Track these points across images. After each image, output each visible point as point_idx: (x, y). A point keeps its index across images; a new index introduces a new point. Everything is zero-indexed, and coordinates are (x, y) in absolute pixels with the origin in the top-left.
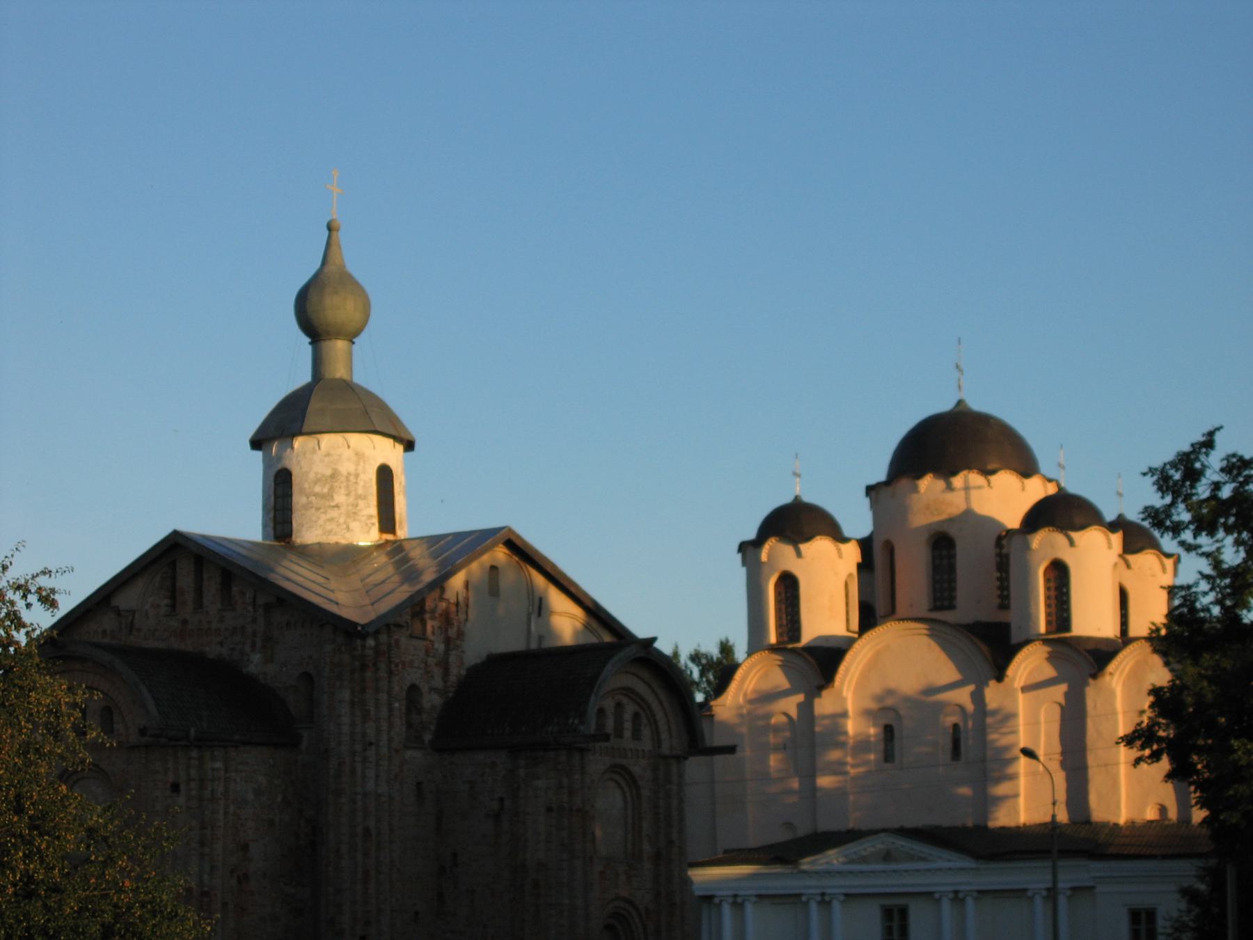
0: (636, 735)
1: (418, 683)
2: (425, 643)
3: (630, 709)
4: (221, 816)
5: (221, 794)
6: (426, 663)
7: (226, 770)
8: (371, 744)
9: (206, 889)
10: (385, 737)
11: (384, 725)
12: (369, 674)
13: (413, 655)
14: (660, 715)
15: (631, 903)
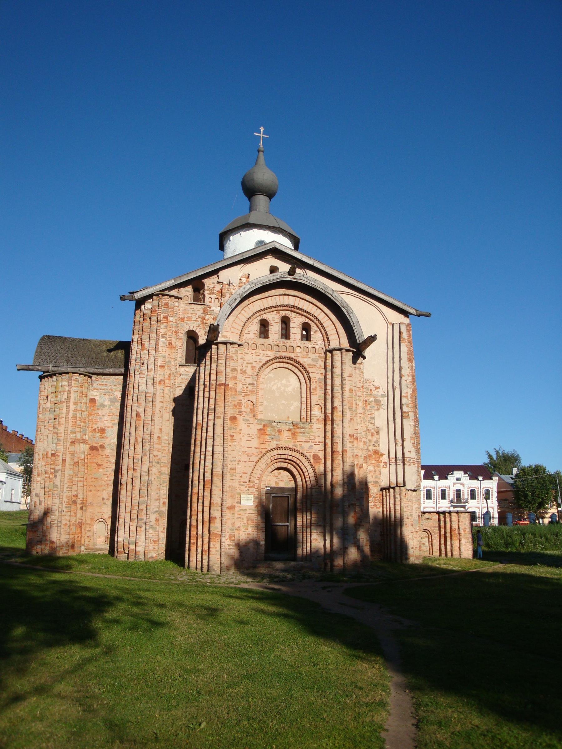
0: (307, 337)
1: (194, 329)
2: (203, 307)
3: (296, 322)
4: (64, 411)
5: (65, 399)
6: (204, 318)
7: (69, 385)
8: (143, 364)
9: (53, 452)
10: (152, 359)
11: (152, 352)
12: (146, 324)
13: (192, 314)
14: (327, 324)
15: (297, 451)
